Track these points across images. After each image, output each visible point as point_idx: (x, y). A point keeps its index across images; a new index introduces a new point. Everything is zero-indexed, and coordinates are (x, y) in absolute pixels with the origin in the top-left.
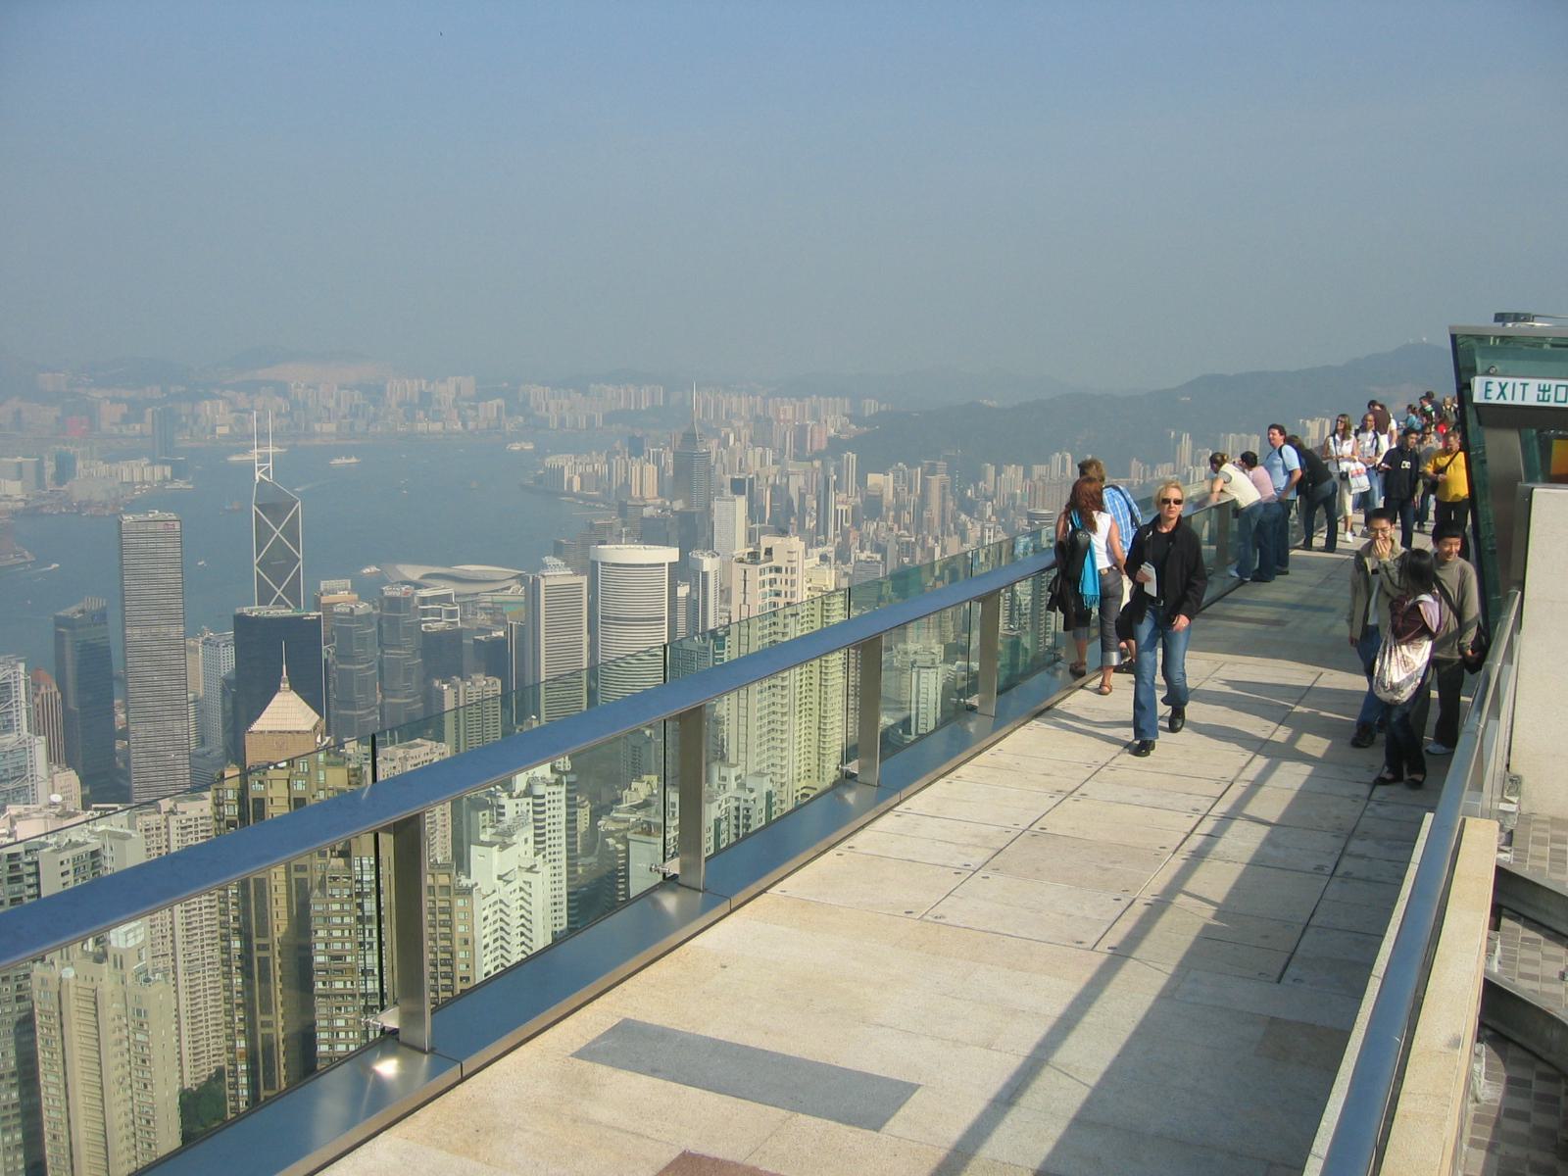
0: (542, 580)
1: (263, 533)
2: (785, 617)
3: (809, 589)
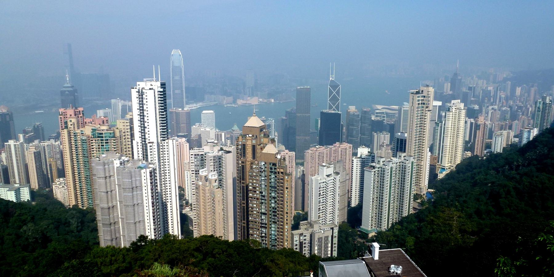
0: (403, 108)
1: (331, 93)
2: (426, 111)
3: (455, 108)
